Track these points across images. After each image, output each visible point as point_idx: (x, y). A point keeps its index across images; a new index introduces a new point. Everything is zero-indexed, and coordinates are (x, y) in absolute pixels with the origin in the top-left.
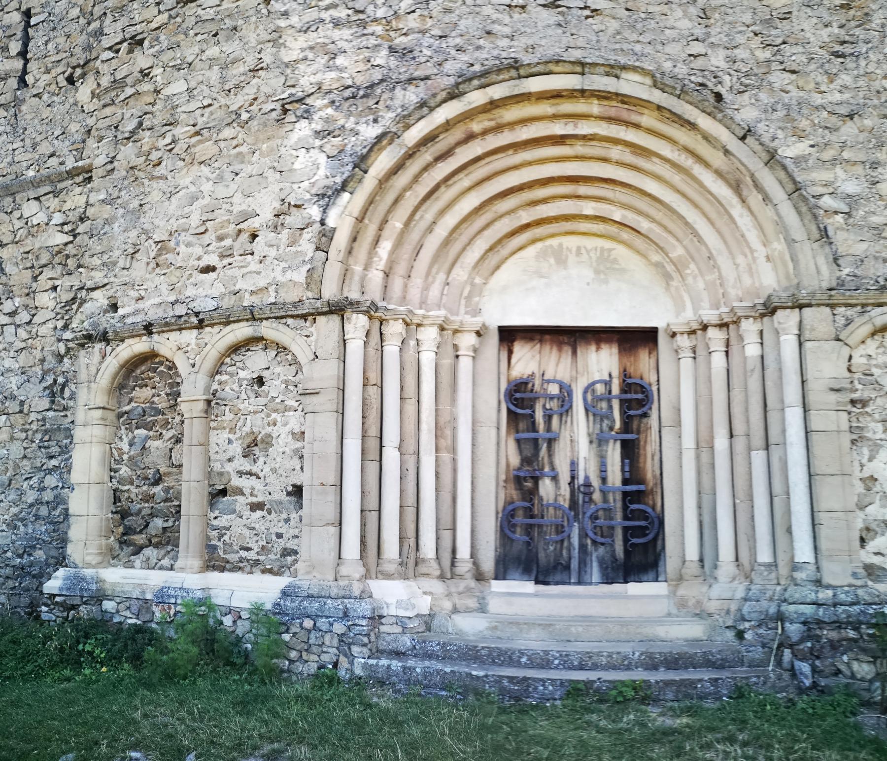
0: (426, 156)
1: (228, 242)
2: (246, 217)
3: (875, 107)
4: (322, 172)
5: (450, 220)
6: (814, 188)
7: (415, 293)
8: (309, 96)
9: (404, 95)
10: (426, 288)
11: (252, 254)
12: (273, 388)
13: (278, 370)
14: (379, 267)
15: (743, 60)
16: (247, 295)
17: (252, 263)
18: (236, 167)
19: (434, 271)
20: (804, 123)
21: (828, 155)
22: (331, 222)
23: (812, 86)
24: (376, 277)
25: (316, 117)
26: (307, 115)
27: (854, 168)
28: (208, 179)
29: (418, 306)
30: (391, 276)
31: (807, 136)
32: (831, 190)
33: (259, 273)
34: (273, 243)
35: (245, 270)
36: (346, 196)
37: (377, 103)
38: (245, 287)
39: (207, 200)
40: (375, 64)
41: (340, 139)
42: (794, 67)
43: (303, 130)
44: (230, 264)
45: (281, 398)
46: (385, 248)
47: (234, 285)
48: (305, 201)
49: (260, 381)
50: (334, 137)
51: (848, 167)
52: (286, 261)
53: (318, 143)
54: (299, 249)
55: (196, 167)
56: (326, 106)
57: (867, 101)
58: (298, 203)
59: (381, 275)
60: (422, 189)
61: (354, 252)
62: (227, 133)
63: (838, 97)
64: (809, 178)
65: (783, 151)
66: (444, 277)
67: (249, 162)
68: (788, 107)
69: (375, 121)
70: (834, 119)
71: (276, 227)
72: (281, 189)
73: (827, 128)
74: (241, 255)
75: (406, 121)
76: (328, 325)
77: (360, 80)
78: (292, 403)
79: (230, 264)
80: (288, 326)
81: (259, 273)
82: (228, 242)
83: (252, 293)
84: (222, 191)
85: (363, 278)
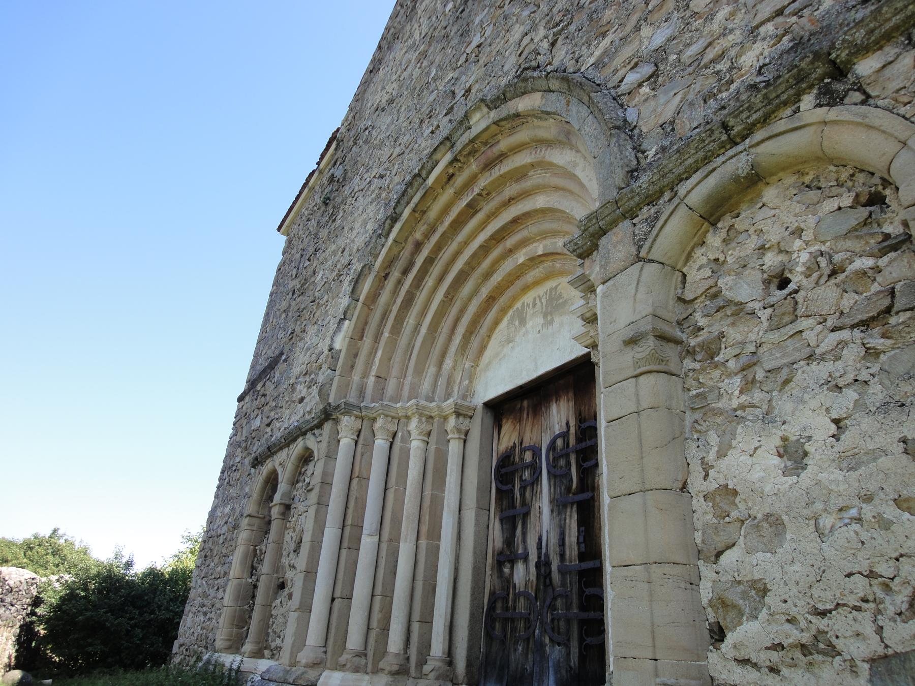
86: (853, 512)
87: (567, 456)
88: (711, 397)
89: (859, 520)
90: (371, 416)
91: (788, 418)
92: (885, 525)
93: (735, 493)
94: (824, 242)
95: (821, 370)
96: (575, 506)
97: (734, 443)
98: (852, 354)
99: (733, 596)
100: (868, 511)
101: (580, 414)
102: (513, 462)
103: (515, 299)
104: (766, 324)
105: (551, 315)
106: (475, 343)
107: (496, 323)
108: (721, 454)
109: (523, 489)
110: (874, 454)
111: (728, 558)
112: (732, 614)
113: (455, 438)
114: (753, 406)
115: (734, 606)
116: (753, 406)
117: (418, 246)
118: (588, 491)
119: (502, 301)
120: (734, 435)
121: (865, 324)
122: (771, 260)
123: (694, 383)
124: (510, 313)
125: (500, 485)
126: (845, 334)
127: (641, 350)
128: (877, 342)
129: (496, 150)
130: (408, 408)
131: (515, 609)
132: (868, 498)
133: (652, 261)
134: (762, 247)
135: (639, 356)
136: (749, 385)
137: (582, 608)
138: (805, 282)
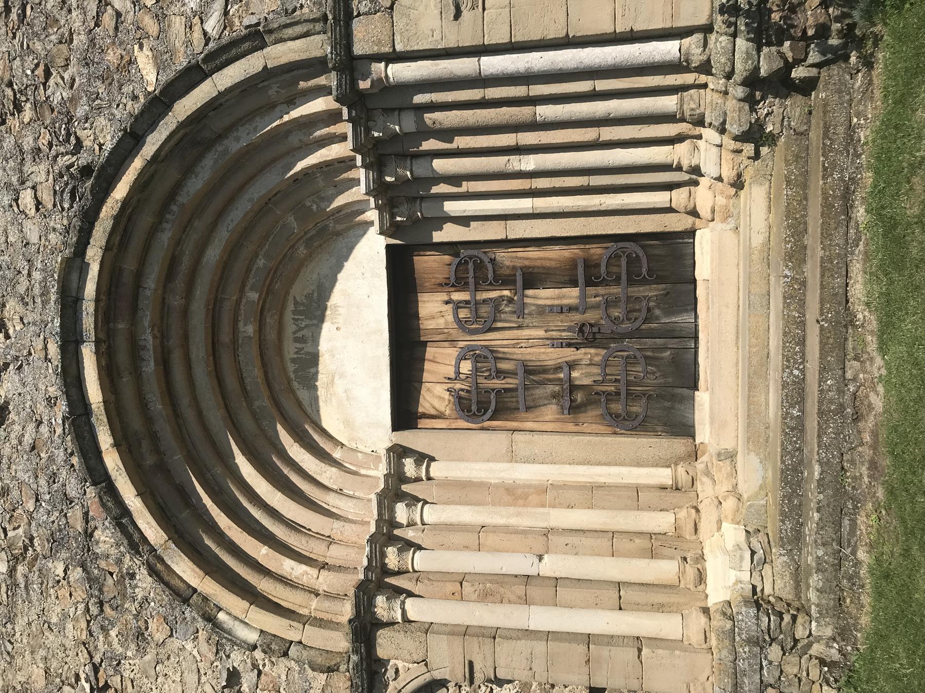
6: (195, 43)
14: (315, 576)
15: (36, 139)
20: (112, 57)
21: (151, 26)
23: (64, 47)
24: (324, 581)
29: (365, 527)
32: (196, 20)
36: (221, 616)
40: (62, 575)
41: (150, 621)
42: (40, 71)
50: (147, 628)
64: (182, 49)
66: (332, 495)
69: (132, 576)
77: (80, 595)
85: (328, 596)
87: (477, 303)
96: (530, 292)
101: (441, 285)
102: (468, 391)
109: (500, 373)
118: (515, 275)
124: (295, 384)
125: (489, 413)
127: (465, 4)
131: (616, 381)
137: (617, 281)
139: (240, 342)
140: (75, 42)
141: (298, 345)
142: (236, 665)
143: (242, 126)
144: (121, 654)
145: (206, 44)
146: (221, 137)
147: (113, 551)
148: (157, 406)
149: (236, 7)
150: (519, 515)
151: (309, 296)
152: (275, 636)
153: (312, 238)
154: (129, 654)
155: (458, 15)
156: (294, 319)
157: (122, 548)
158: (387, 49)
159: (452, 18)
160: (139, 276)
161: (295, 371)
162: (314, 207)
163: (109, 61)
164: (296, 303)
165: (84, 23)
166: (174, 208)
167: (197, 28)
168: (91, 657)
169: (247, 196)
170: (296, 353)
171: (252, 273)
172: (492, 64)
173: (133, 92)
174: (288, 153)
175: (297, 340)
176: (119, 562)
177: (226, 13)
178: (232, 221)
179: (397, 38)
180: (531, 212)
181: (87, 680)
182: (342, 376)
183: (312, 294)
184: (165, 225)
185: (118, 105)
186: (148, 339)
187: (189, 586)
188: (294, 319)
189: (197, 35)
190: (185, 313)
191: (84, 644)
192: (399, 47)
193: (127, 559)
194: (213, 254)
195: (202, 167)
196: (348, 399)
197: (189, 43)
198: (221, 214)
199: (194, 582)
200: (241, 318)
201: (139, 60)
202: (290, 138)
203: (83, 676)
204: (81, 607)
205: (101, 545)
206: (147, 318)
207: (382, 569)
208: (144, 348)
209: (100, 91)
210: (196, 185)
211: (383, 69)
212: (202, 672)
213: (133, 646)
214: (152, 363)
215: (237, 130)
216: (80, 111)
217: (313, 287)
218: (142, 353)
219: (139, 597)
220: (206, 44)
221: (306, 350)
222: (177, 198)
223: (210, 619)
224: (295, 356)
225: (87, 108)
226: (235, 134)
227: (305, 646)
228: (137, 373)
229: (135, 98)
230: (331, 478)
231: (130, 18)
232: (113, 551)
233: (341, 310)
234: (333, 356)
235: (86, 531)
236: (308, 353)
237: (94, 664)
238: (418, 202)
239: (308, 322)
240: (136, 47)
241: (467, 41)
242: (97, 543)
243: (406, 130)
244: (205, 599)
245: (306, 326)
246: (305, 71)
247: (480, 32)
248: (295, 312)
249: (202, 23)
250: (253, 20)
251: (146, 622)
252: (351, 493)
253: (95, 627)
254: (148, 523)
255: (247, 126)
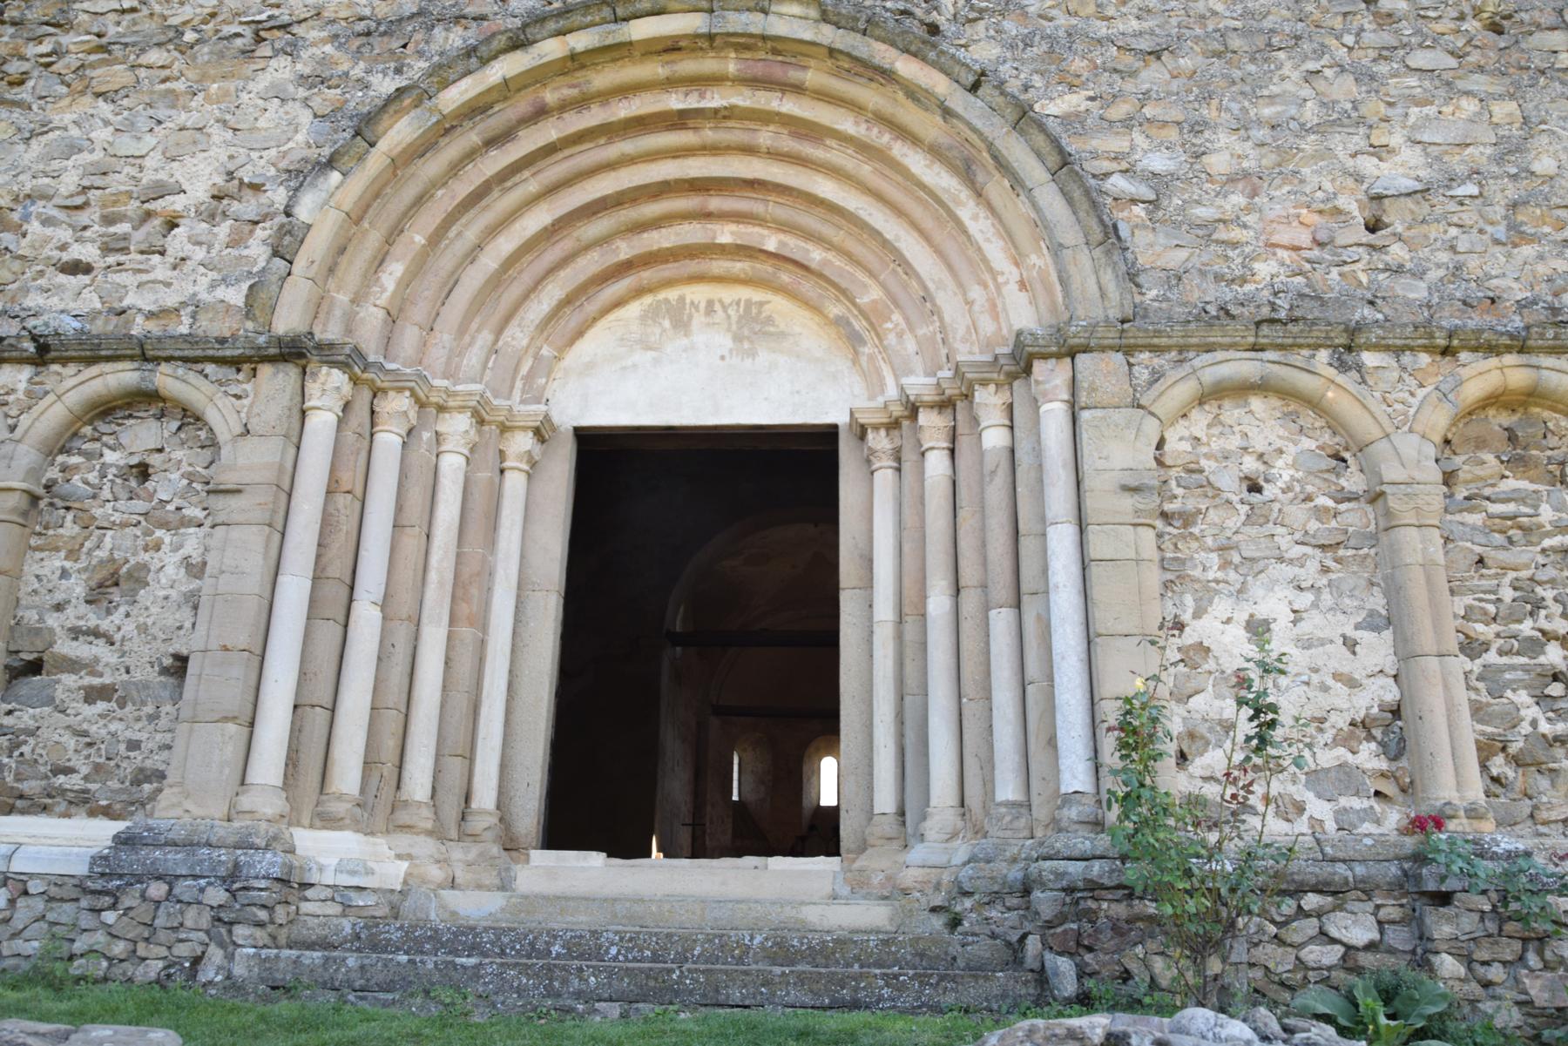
0: (472, 137)
1: (123, 228)
2: (161, 191)
3: (1197, 39)
4: (300, 137)
5: (506, 244)
7: (437, 355)
8: (300, 22)
9: (447, 38)
10: (457, 353)
11: (162, 253)
12: (165, 486)
13: (178, 454)
14: (378, 302)
16: (139, 319)
17: (159, 268)
18: (161, 113)
19: (474, 326)
20: (1078, 65)
21: (1119, 111)
22: (303, 212)
25: (305, 54)
26: (291, 51)
27: (1164, 132)
28: (107, 123)
30: (398, 322)
31: (1083, 83)
33: (168, 285)
34: (203, 238)
35: (145, 277)
36: (335, 177)
37: (404, 46)
38: (140, 303)
39: (98, 155)
41: (338, 91)
43: (281, 70)
44: (119, 264)
45: (177, 502)
46: (394, 272)
47: (121, 301)
48: (268, 179)
49: (143, 472)
50: (329, 88)
51: (1153, 132)
52: (220, 270)
53: (302, 93)
54: (245, 252)
55: (88, 99)
56: (324, 41)
57: (1183, 31)
58: (256, 181)
59: (381, 314)
60: (463, 188)
61: (339, 273)
62: (154, 56)
63: (1135, 24)
64: (1088, 148)
65: (1043, 106)
67: (184, 108)
68: (1051, 39)
69: (398, 71)
70: (1128, 60)
71: (213, 216)
72: (231, 157)
73: (1116, 71)
74: (142, 252)
75: (443, 74)
76: (275, 382)
78: (195, 512)
79: (119, 264)
80: (206, 376)
81: (168, 285)
82: (123, 228)
83: (151, 315)
84: (126, 145)
86: (1305, 678)
88: (1189, 564)
89: (1307, 684)
90: (379, 383)
91: (1258, 600)
92: (1325, 688)
93: (1208, 650)
94: (1297, 470)
95: (1289, 571)
97: (1210, 609)
98: (1313, 566)
99: (1203, 729)
100: (1315, 678)
103: (669, 283)
104: (1243, 518)
105: (752, 342)
106: (572, 320)
107: (619, 303)
108: (1197, 615)
110: (1322, 642)
111: (1195, 702)
112: (1199, 743)
113: (520, 470)
114: (1227, 582)
115: (1202, 737)
116: (1227, 582)
117: (541, 113)
119: (647, 275)
120: (1211, 602)
121: (1323, 547)
122: (1250, 465)
123: (1171, 547)
124: (648, 300)
126: (1308, 550)
128: (1330, 563)
129: (794, 75)
130: (455, 394)
132: (1316, 670)
133: (1153, 414)
134: (1245, 449)
135: (1141, 507)
136: (1225, 565)
138: (1281, 496)
139: (709, 226)
140: (1098, 23)
141: (703, 306)
142: (269, 194)
143: (993, 225)
144: (299, 56)
145: (1094, 176)
146: (979, 194)
147: (434, 47)
148: (624, 110)
149: (1143, 214)
150: (441, 584)
151: (770, 320)
152: (302, 242)
153: (849, 324)
154: (299, 66)
155: (1127, 489)
156: (740, 300)
157: (436, 58)
158: (1083, 398)
159: (1123, 482)
160: (798, 89)
161: (667, 301)
162: (889, 325)
163: (1073, 60)
164: (761, 304)
165: (1123, 34)
166: (886, 138)
167: (1114, 166)
168: (300, 22)
169: (902, 233)
170: (692, 303)
171: (803, 244)
172: (1062, 541)
173: (1032, 87)
174: (960, 285)
175: (710, 303)
176: (420, 54)
177: (1134, 201)
178: (870, 214)
179: (1099, 413)
180: (875, 619)
181: (271, 17)
182: (656, 361)
183: (773, 325)
184: (864, 126)
185: (1017, 69)
186: (715, 99)
187: (379, 138)
188: (740, 300)
189: (1106, 166)
190: (749, 150)
191: (318, 14)
192: (1085, 415)
193: (423, 64)
194: (826, 188)
195: (938, 174)
196: (624, 368)
197: (1095, 156)
198: (878, 196)
199: (383, 145)
200: (742, 228)
201: (1075, 96)
202: (977, 287)
203: (276, 12)
204: (367, 12)
205: (444, 34)
206: (742, 98)
207: (379, 389)
208: (702, 96)
209: (1035, 49)
210: (917, 162)
211: (1060, 397)
212: (265, 153)
213: (307, 71)
214: (681, 106)
215: (987, 218)
216: (1011, 27)
217: (782, 327)
218: (696, 94)
219: (371, 78)
220: (1094, 176)
221: (696, 315)
222: (899, 142)
223: (331, 163)
224: (688, 301)
225: (1014, 33)
226: (982, 215)
227: (283, 280)
228: (670, 83)
229: (1026, 88)
230: (513, 339)
231: (1129, 86)
232: (434, 47)
233: (748, 362)
234: (685, 350)
235: (465, 17)
236: (690, 317)
237: (290, 25)
238: (895, 465)
239: (734, 318)
240: (1091, 93)
241: (1090, 503)
242: (447, 30)
243: (985, 435)
244: (361, 158)
245: (729, 317)
246: (1060, 299)
247: (1105, 520)
248: (749, 303)
249: (1121, 171)
250: (1124, 231)
251: (337, 86)
252: (490, 364)
253: (335, 29)
254: (466, 90)
255: (992, 230)
